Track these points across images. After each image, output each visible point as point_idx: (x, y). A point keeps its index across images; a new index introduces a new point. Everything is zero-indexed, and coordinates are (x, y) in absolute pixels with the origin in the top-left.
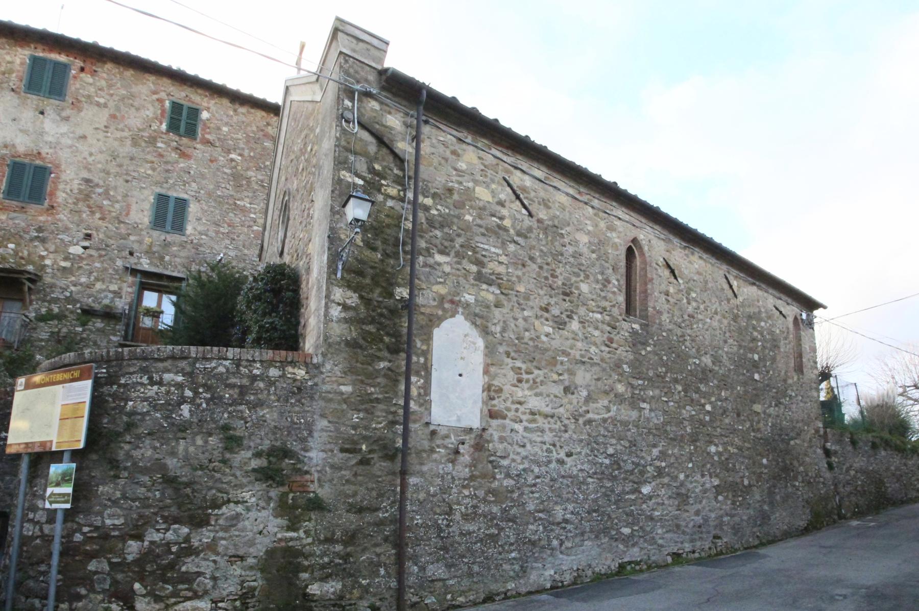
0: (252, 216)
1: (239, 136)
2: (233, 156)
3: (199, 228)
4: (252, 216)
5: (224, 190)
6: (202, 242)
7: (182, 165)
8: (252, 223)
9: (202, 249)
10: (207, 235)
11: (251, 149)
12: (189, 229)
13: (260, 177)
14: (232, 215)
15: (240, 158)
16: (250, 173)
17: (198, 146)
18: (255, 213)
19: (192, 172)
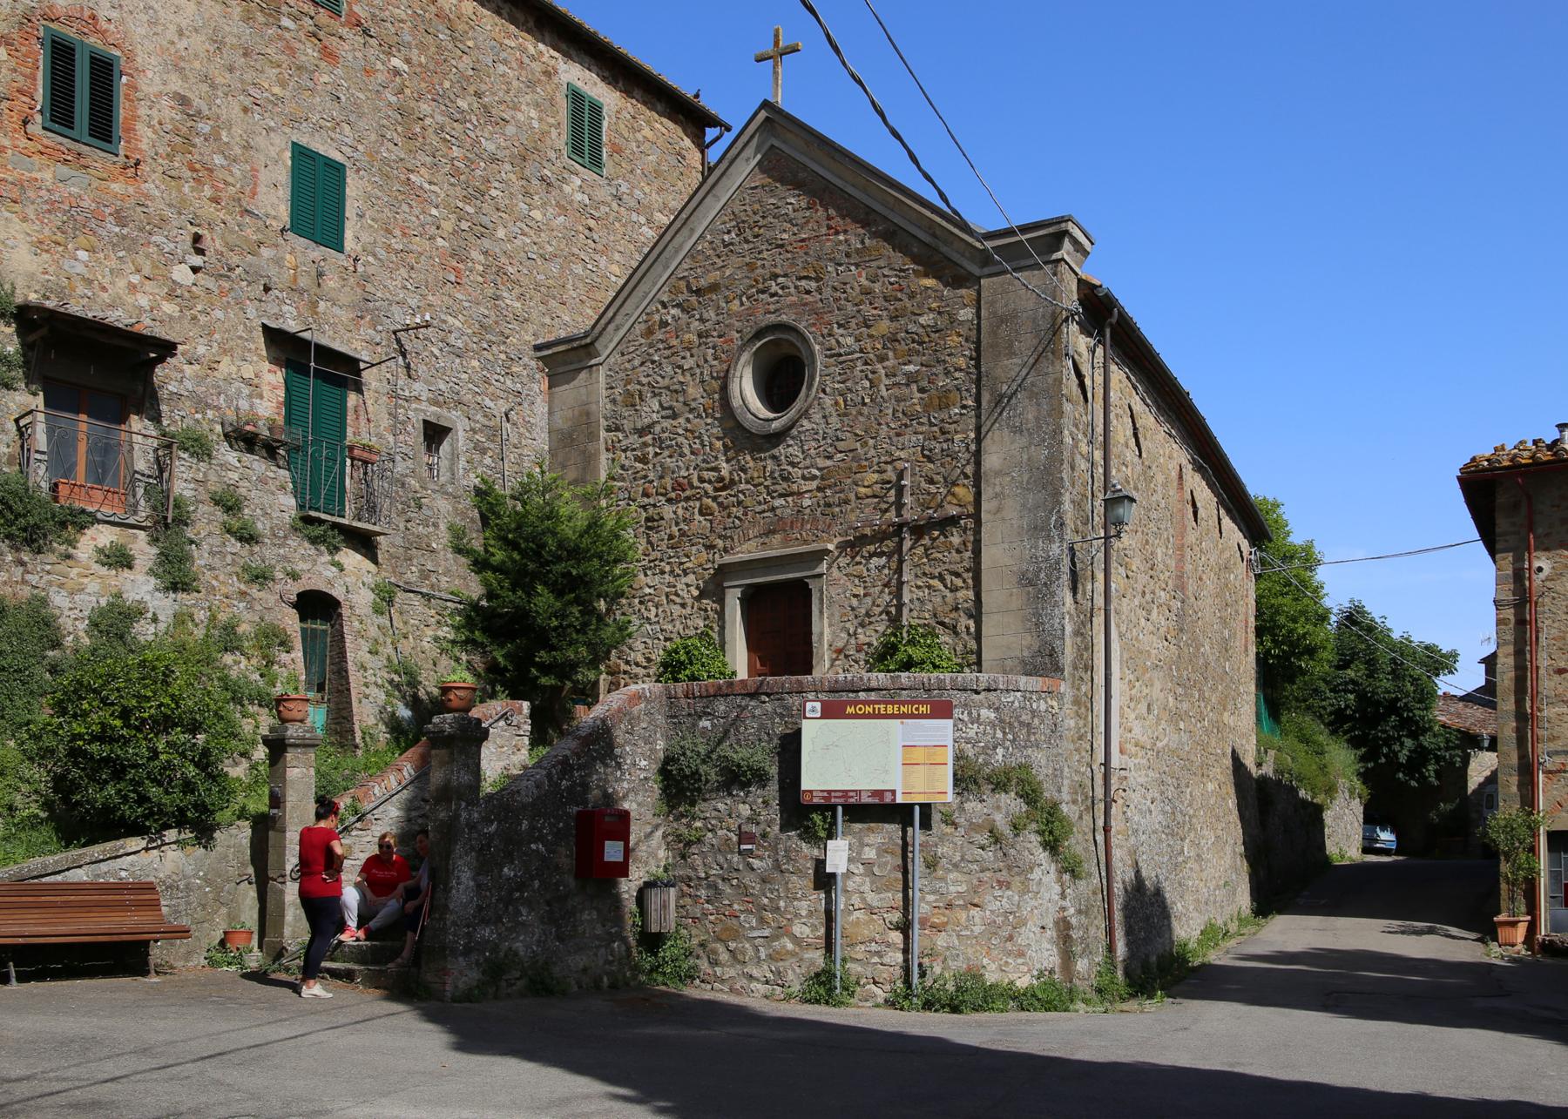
0: (434, 212)
1: (404, 16)
2: (396, 62)
3: (365, 238)
4: (434, 212)
5: (391, 146)
6: (371, 270)
7: (326, 78)
8: (433, 230)
9: (372, 290)
10: (374, 255)
11: (422, 47)
12: (349, 243)
13: (440, 118)
14: (405, 208)
15: (406, 67)
16: (425, 108)
17: (344, 31)
18: (437, 207)
19: (343, 98)
